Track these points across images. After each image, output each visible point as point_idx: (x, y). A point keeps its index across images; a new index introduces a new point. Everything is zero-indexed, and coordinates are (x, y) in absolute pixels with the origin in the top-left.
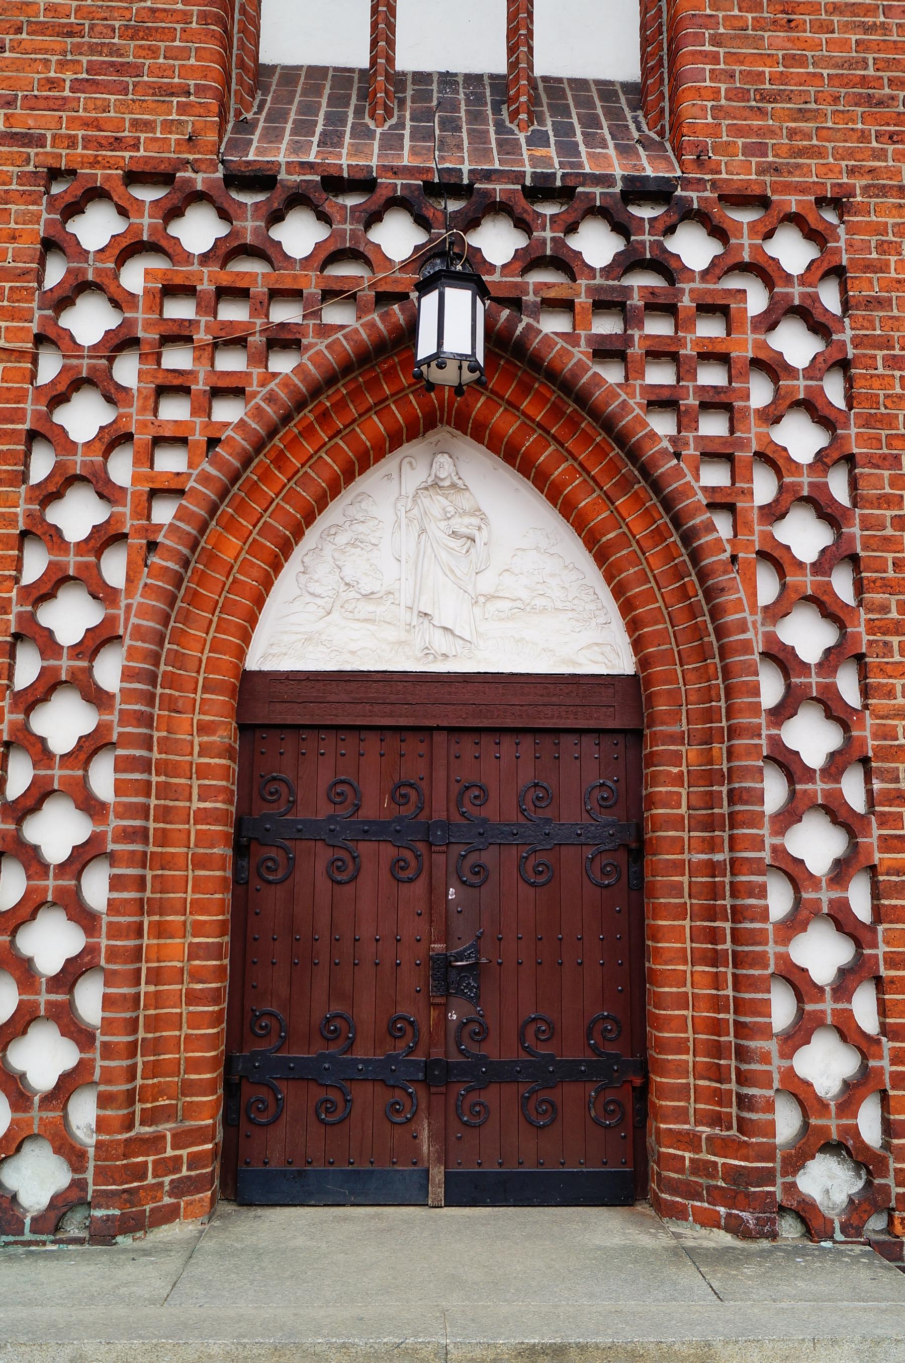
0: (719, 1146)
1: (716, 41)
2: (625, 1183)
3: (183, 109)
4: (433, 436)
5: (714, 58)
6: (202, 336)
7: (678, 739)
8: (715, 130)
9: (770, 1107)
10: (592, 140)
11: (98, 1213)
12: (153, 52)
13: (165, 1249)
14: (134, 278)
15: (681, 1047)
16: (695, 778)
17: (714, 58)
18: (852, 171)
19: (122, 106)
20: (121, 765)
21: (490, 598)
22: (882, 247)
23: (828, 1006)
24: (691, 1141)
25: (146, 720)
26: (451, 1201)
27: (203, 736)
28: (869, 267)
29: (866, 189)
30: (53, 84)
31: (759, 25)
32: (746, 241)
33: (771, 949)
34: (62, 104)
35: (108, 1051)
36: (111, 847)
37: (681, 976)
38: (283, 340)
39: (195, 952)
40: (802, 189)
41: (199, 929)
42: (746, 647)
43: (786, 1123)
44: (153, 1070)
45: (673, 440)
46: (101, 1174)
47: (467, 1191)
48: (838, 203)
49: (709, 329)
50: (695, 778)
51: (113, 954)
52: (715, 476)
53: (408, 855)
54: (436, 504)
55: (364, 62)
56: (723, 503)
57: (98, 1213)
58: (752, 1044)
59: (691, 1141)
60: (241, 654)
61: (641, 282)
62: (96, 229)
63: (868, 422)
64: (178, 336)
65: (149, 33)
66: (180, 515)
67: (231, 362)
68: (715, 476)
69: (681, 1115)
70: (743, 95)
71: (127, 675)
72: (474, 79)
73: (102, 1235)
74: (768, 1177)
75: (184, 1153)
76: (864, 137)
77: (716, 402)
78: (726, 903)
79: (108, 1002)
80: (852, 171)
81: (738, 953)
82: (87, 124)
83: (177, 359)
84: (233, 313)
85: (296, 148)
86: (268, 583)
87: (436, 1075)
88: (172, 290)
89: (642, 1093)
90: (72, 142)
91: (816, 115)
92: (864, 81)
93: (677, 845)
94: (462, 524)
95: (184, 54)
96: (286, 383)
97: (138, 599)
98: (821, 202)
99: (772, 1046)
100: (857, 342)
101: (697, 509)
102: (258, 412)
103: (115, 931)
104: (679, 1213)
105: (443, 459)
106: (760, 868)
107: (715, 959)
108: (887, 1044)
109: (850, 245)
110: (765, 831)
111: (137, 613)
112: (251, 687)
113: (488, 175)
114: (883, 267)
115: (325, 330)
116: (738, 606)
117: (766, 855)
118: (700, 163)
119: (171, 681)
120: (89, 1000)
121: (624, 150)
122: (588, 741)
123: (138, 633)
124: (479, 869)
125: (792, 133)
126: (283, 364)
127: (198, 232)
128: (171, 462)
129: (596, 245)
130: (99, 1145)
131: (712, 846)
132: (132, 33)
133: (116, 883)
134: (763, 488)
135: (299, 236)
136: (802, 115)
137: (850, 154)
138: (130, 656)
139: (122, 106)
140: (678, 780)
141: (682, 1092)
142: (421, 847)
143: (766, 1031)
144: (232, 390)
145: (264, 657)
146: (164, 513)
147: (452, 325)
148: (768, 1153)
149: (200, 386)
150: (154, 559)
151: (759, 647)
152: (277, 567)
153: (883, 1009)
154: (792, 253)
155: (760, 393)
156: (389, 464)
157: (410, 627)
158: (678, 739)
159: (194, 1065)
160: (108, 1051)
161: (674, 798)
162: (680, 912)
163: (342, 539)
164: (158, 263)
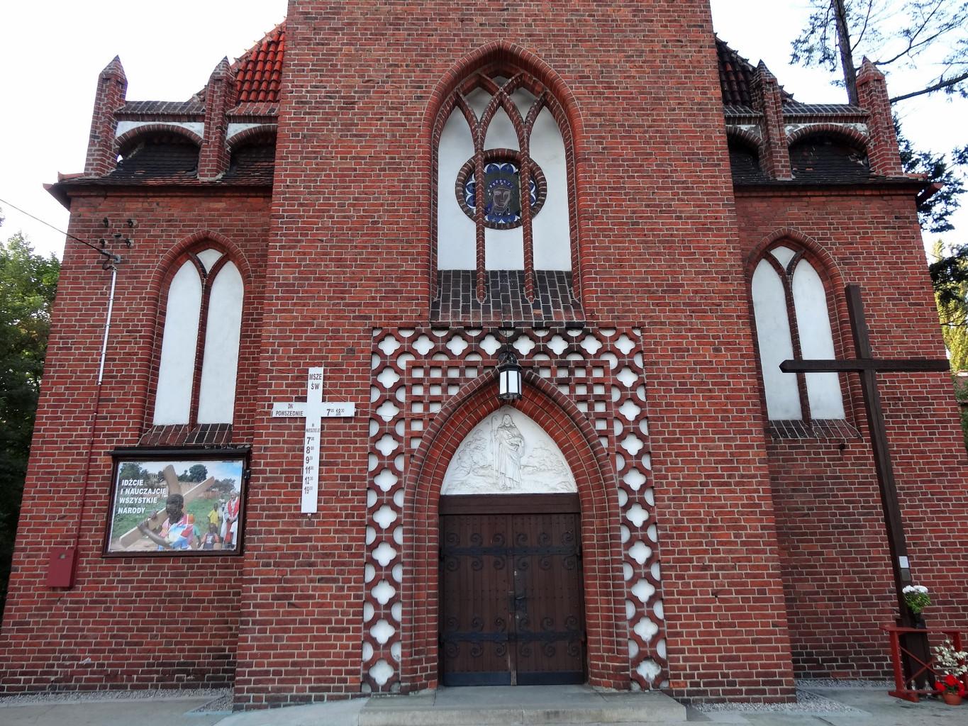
0: (611, 659)
1: (596, 273)
2: (579, 676)
3: (417, 305)
4: (502, 409)
5: (595, 279)
6: (426, 383)
7: (592, 517)
8: (597, 305)
9: (627, 645)
10: (556, 305)
11: (403, 684)
12: (406, 286)
13: (422, 697)
14: (402, 363)
15: (597, 626)
16: (599, 531)
17: (595, 279)
18: (644, 317)
19: (397, 305)
20: (405, 532)
21: (525, 466)
22: (655, 344)
23: (645, 609)
24: (601, 658)
25: (411, 516)
26: (519, 684)
27: (429, 520)
28: (651, 351)
29: (649, 323)
30: (374, 298)
31: (611, 267)
32: (609, 343)
33: (625, 590)
34: (377, 305)
35: (404, 629)
36: (403, 560)
37: (596, 601)
38: (453, 382)
39: (429, 596)
40: (627, 324)
41: (430, 588)
42: (613, 485)
43: (633, 650)
44: (417, 636)
45: (586, 414)
46: (404, 671)
47: (524, 680)
48: (640, 327)
49: (598, 374)
50: (599, 531)
51: (405, 597)
52: (601, 425)
53: (500, 560)
54: (505, 433)
55: (475, 268)
56: (603, 434)
57: (403, 684)
58: (620, 623)
59: (601, 658)
60: (439, 489)
62: (389, 346)
63: (653, 405)
64: (418, 382)
65: (405, 279)
66: (421, 445)
67: (436, 391)
68: (601, 425)
69: (598, 650)
70: (606, 292)
71: (406, 501)
72: (512, 273)
73: (404, 692)
74: (626, 669)
75: (429, 665)
76: (648, 305)
77: (600, 399)
78: (610, 574)
79: (404, 613)
80: (644, 317)
81: (620, 593)
82: (385, 311)
83: (418, 391)
84: (436, 374)
85: (455, 315)
86: (447, 464)
87: (513, 638)
88: (415, 366)
89: (585, 643)
90: (380, 318)
91: (632, 298)
92: (647, 285)
93: (593, 554)
94: (515, 441)
95: (416, 286)
96: (455, 398)
97: (408, 475)
98: (634, 328)
99: (626, 623)
100: (648, 377)
101: (595, 438)
102: (445, 410)
103: (405, 589)
104: (598, 684)
105: (507, 417)
106: (621, 562)
107: (608, 594)
108: (666, 622)
109: (644, 343)
110: (622, 549)
111: (408, 480)
112: (445, 501)
113: (520, 324)
114: (656, 351)
115: (467, 380)
116: (610, 471)
117: (622, 557)
118: (592, 317)
119: (418, 502)
120: (397, 612)
121: (567, 309)
122: (562, 517)
123: (409, 486)
124: (524, 564)
125: (623, 305)
126: (453, 391)
127: (424, 346)
128: (417, 426)
129: (558, 346)
130: (402, 662)
131: (605, 554)
132: (398, 279)
133: (405, 572)
134: (618, 428)
135: (458, 346)
136: (626, 298)
137: (644, 311)
138: (407, 494)
139: (397, 305)
140: (593, 531)
141: (598, 642)
142: (504, 556)
143: (624, 618)
144: (436, 400)
145: (447, 490)
146: (416, 444)
147: (510, 383)
148: (626, 660)
149: (426, 401)
150: (413, 461)
151: (617, 485)
152: (450, 457)
153: (665, 610)
154: (625, 346)
155: (616, 395)
156: (488, 419)
157: (497, 478)
158: (592, 517)
159: (430, 635)
160: (404, 629)
161: (591, 538)
162: (595, 578)
163: (472, 446)
164: (411, 358)
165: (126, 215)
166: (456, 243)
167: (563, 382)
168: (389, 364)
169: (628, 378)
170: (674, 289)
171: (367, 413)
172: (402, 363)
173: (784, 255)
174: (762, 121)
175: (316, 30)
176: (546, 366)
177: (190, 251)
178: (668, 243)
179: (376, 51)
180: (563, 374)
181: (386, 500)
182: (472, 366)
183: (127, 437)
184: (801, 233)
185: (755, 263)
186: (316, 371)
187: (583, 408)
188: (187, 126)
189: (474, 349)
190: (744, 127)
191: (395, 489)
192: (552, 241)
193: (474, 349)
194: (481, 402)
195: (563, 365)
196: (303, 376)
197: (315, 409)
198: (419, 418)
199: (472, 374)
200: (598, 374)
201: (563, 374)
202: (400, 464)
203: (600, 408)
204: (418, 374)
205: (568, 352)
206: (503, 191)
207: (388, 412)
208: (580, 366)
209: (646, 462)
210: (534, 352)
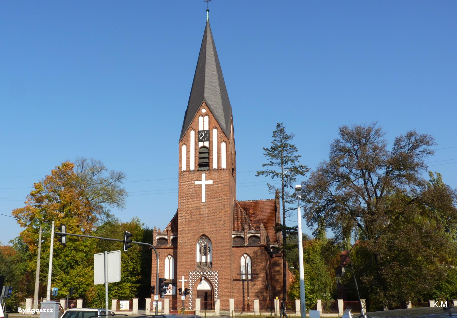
147: (203, 278)
154: (216, 273)
170: (222, 266)
171: (189, 281)
173: (245, 255)
177: (167, 256)
178: (222, 261)
179: (189, 235)
184: (247, 253)
185: (241, 257)
189: (200, 274)
193: (200, 274)
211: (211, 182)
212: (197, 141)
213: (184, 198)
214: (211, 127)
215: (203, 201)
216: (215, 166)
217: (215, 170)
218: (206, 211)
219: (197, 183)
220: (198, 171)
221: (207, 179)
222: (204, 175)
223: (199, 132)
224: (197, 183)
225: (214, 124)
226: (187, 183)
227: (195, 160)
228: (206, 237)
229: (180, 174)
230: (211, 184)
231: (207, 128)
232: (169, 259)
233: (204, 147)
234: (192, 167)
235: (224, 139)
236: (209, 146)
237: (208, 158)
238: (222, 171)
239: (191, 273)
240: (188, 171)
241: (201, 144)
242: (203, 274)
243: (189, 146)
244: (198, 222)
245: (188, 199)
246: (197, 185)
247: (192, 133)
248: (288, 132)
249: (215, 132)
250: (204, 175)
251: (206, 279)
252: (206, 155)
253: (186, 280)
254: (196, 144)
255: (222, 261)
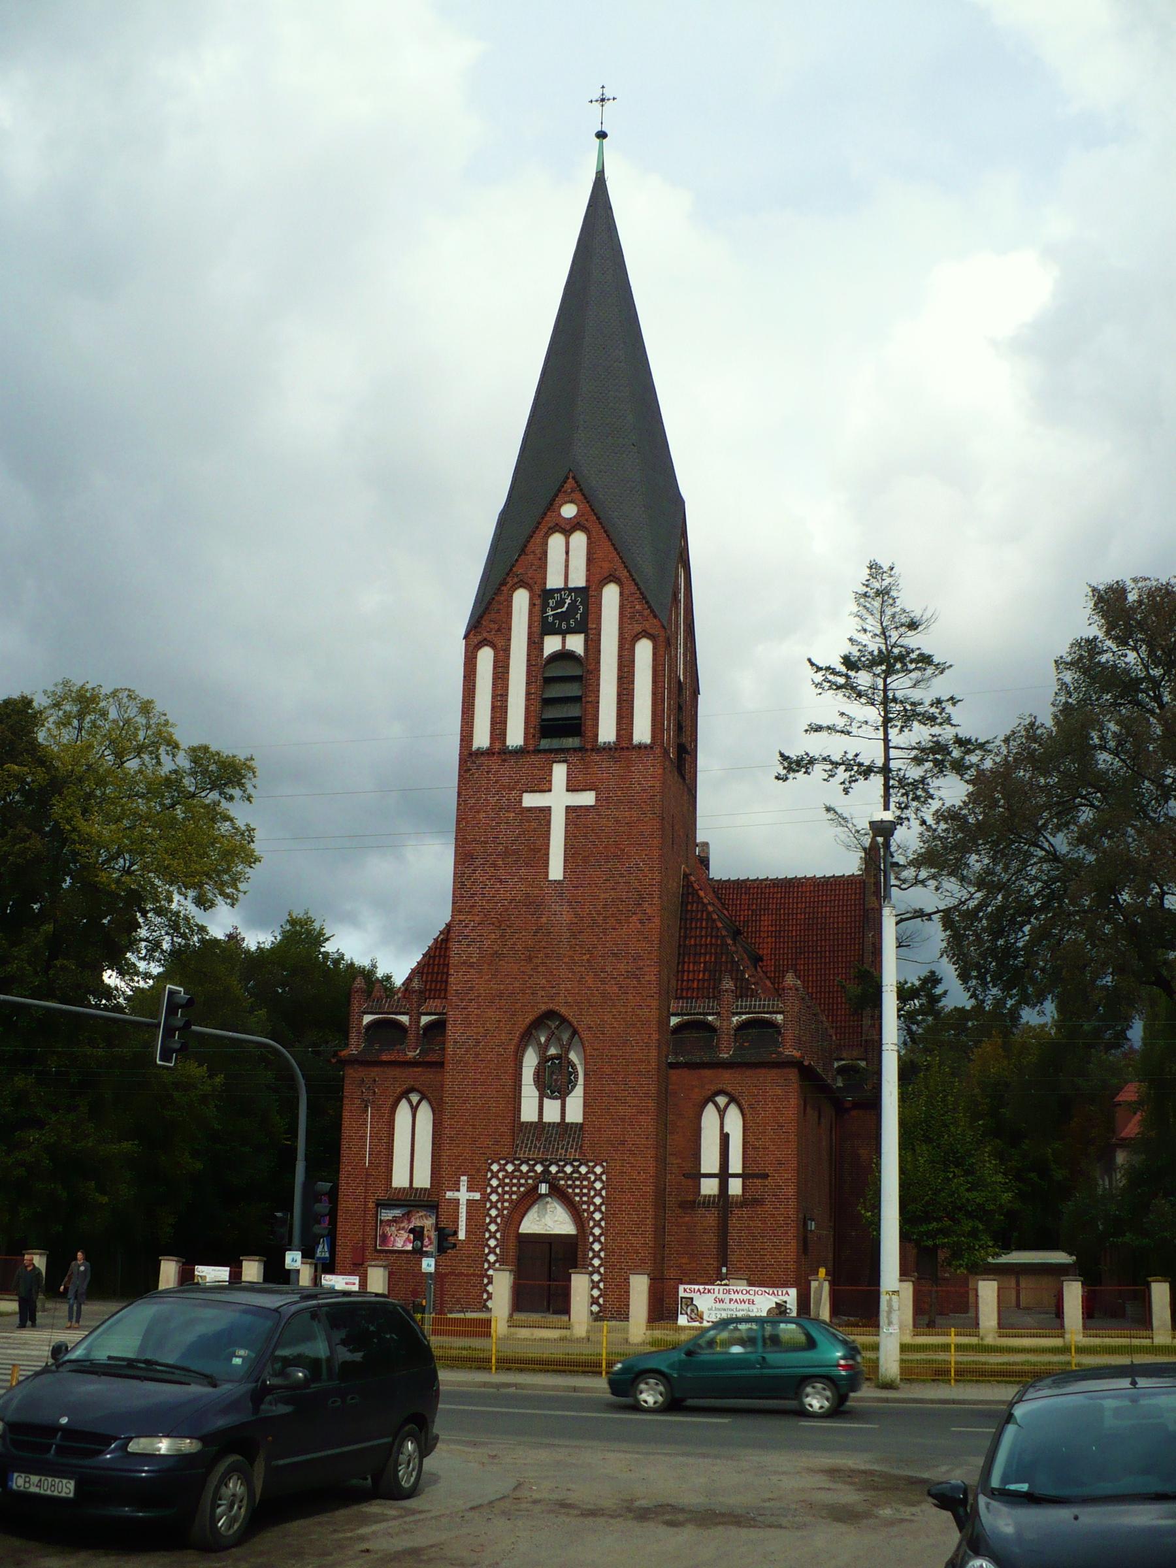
27: (512, 1244)
38: (522, 1185)
48: (606, 1161)
49: (585, 1183)
52: (585, 1207)
56: (585, 1210)
61: (575, 1175)
62: (495, 1167)
64: (507, 1184)
67: (515, 1189)
68: (585, 1207)
77: (585, 1195)
83: (507, 1189)
84: (515, 1181)
126: (522, 1189)
127: (510, 1168)
128: (506, 1204)
134: (592, 1208)
135: (524, 1168)
144: (514, 1193)
147: (543, 1188)
155: (592, 1193)
165: (373, 1074)
166: (528, 1113)
167: (570, 1186)
168: (495, 1175)
169: (598, 1185)
170: (623, 1143)
172: (501, 1175)
174: (718, 1014)
175: (462, 1000)
176: (562, 1179)
177: (405, 1094)
178: (623, 1120)
180: (570, 1182)
181: (492, 1236)
182: (531, 1178)
183: (381, 1195)
184: (729, 1089)
186: (464, 1178)
187: (577, 1199)
188: (399, 1017)
190: (710, 1018)
191: (497, 1231)
192: (575, 1111)
194: (530, 1198)
195: (569, 1179)
196: (458, 1183)
197: (463, 1195)
198: (506, 1201)
199: (530, 1181)
200: (585, 1183)
201: (570, 1182)
202: (499, 1220)
203: (585, 1199)
204: (507, 1181)
205: (573, 1172)
206: (554, 1082)
207: (494, 1198)
208: (577, 1179)
209: (603, 1224)
210: (558, 1172)
211: (587, 799)
212: (537, 630)
213: (478, 862)
214: (597, 579)
215: (551, 877)
216: (607, 732)
217: (607, 748)
218: (564, 915)
219: (531, 800)
220: (537, 751)
221: (571, 788)
222: (560, 772)
223: (549, 594)
224: (531, 800)
225: (606, 565)
226: (493, 800)
227: (527, 708)
228: (563, 1020)
229: (463, 761)
230: (587, 808)
231: (578, 579)
232: (414, 1110)
233: (564, 656)
234: (515, 737)
235: (647, 625)
236: (586, 650)
237: (577, 699)
238: (634, 755)
239: (495, 1167)
240: (498, 749)
241: (552, 644)
242: (546, 1171)
243: (507, 650)
244: (530, 959)
245: (494, 865)
246: (530, 809)
247: (521, 600)
248: (909, 601)
249: (611, 595)
250: (560, 772)
251: (558, 1192)
252: (572, 690)
253: (477, 1196)
254: (535, 645)
255: (623, 1120)
